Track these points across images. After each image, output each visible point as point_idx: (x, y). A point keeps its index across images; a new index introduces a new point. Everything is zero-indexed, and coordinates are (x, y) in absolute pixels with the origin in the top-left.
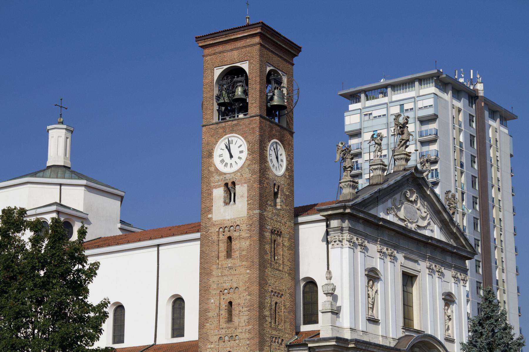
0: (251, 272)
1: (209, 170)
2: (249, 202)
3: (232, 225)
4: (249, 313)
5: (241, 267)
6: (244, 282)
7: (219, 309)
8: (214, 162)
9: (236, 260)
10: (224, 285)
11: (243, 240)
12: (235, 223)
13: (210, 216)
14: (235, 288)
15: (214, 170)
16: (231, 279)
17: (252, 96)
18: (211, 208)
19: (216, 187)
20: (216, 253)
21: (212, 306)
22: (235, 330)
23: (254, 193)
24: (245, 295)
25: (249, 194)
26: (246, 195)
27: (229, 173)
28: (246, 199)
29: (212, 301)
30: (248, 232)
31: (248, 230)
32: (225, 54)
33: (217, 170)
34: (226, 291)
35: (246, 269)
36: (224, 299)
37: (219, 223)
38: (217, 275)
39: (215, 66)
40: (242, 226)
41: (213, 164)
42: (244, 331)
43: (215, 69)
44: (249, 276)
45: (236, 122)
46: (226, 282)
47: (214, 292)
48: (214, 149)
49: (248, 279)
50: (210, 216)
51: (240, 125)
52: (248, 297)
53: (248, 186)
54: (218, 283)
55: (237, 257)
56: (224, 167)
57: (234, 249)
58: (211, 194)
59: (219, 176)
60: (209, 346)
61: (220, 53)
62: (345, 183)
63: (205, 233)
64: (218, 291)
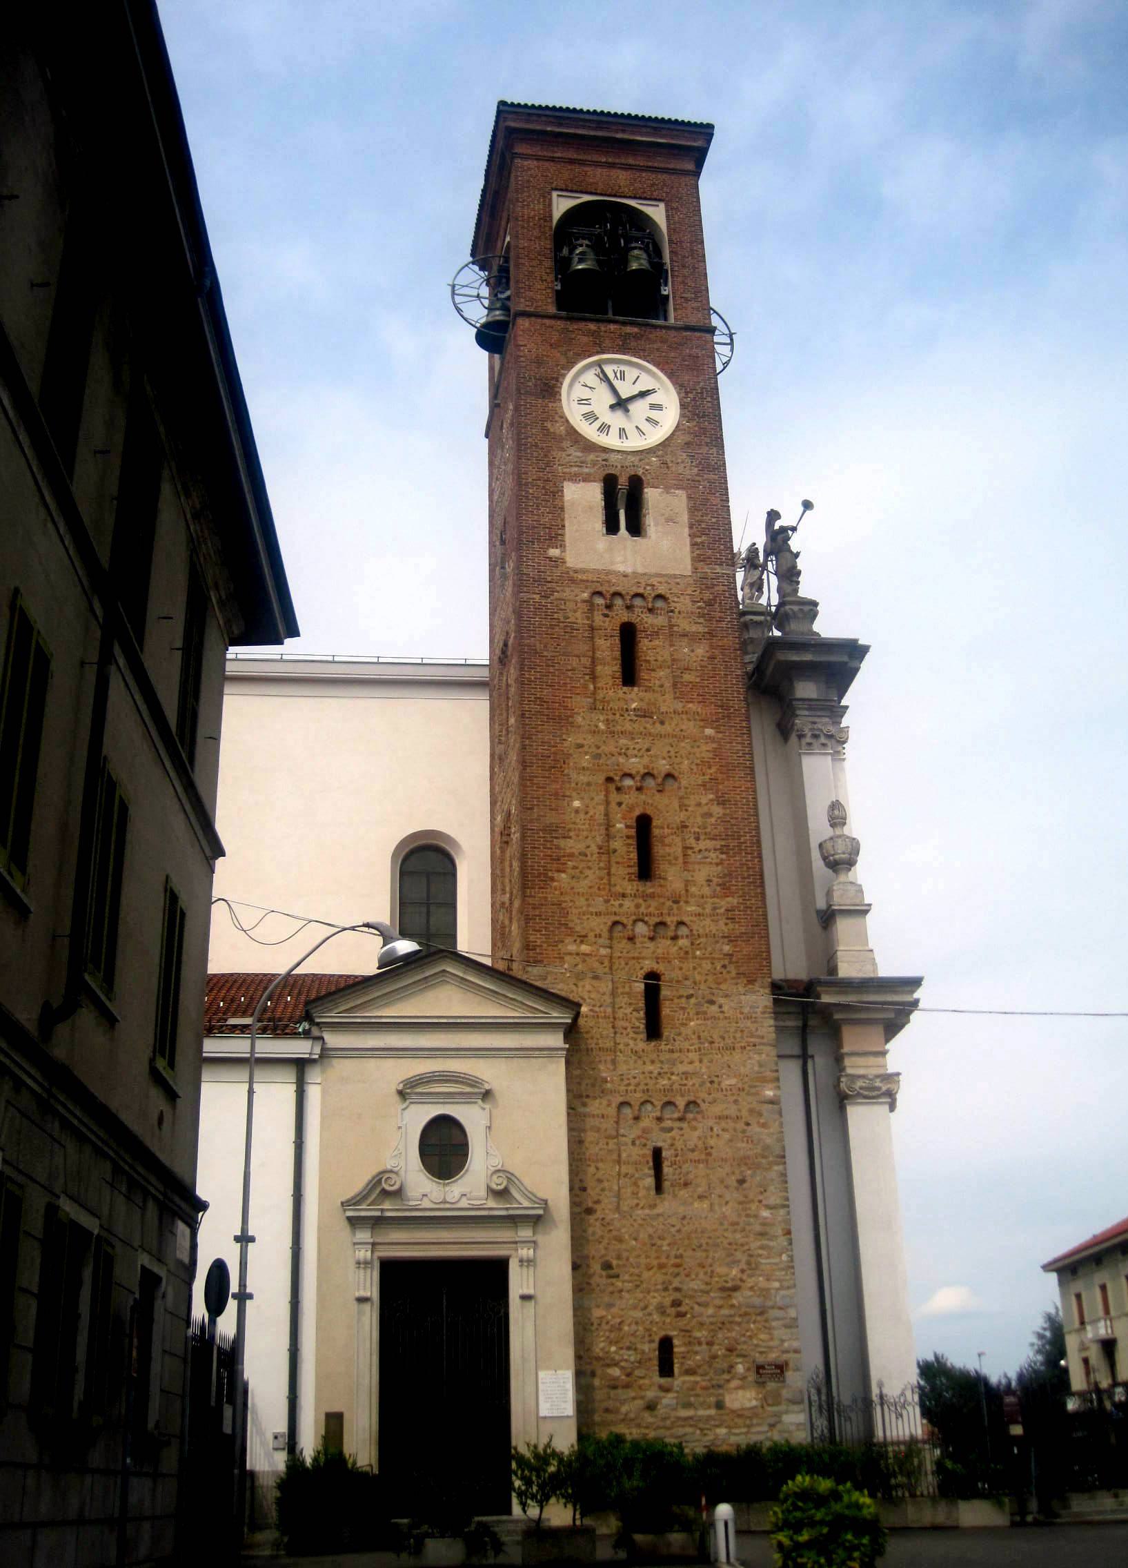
0: (720, 735)
1: (544, 428)
2: (699, 540)
3: (641, 591)
4: (724, 856)
5: (684, 716)
6: (698, 761)
7: (603, 831)
8: (563, 412)
9: (656, 695)
10: (621, 760)
11: (686, 639)
12: (649, 588)
13: (554, 552)
14: (663, 775)
15: (563, 432)
16: (646, 747)
17: (683, 282)
18: (560, 532)
19: (574, 478)
20: (586, 661)
21: (578, 821)
22: (675, 906)
23: (714, 520)
24: (704, 801)
25: (697, 519)
26: (685, 518)
27: (619, 451)
28: (686, 531)
29: (577, 804)
30: (701, 620)
31: (701, 616)
32: (586, 169)
33: (574, 436)
34: (628, 782)
35: (702, 724)
36: (620, 804)
37: (590, 578)
38: (593, 728)
39: (554, 185)
40: (676, 599)
41: (562, 417)
42: (708, 910)
43: (555, 194)
44: (715, 745)
45: (636, 330)
46: (630, 752)
47: (583, 778)
48: (561, 380)
49: (711, 755)
50: (554, 552)
51: (648, 339)
52: (717, 810)
53: (689, 498)
54: (599, 751)
55: (662, 686)
56: (599, 433)
57: (648, 661)
58: (557, 493)
59: (582, 452)
60: (572, 948)
61: (572, 162)
62: (801, 607)
63: (537, 597)
64: (600, 778)
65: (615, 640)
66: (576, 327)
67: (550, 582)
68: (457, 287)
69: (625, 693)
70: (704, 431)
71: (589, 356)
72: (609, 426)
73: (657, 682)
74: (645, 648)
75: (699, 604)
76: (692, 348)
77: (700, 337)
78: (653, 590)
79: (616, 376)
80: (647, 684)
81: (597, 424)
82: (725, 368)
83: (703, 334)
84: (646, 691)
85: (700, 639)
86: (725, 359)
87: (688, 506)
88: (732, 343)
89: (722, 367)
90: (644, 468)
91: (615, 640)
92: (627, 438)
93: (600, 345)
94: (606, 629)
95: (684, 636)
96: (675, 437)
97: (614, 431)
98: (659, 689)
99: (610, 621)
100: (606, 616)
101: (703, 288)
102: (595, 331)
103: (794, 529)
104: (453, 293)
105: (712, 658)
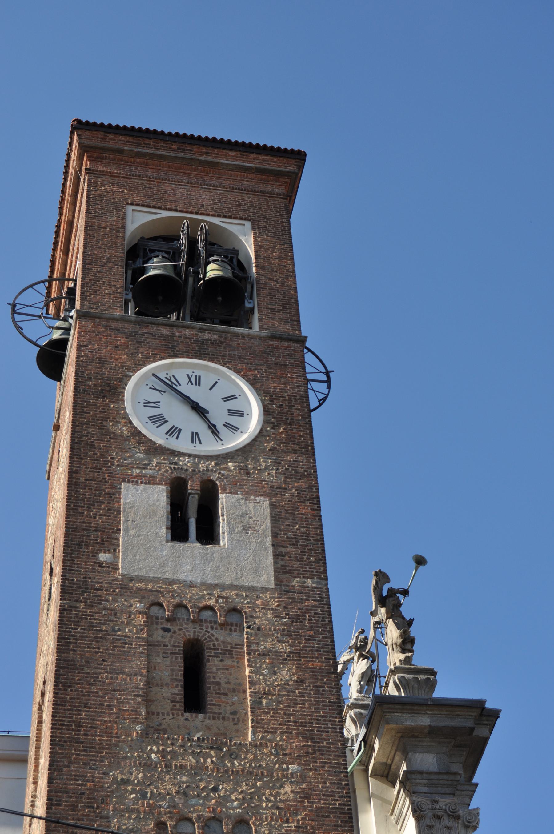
17: (270, 294)
19: (134, 480)
31: (288, 633)
43: (130, 208)
48: (125, 380)
53: (272, 506)
56: (167, 436)
57: (219, 684)
65: (176, 658)
66: (145, 331)
67: (98, 590)
68: (18, 307)
69: (186, 719)
70: (291, 438)
71: (160, 360)
72: (180, 430)
73: (228, 708)
74: (214, 669)
75: (285, 620)
76: (279, 356)
77: (289, 347)
78: (227, 602)
79: (190, 381)
80: (215, 709)
81: (166, 427)
82: (320, 405)
83: (291, 344)
84: (214, 718)
85: (285, 660)
86: (321, 396)
87: (271, 514)
88: (328, 381)
89: (318, 404)
90: (220, 473)
91: (176, 658)
92: (200, 443)
93: (173, 349)
94: (167, 646)
95: (264, 655)
96: (257, 443)
97: (186, 436)
98: (231, 717)
99: (171, 637)
100: (167, 630)
101: (293, 300)
102: (168, 335)
103: (405, 592)
104: (14, 312)
105: (300, 681)
